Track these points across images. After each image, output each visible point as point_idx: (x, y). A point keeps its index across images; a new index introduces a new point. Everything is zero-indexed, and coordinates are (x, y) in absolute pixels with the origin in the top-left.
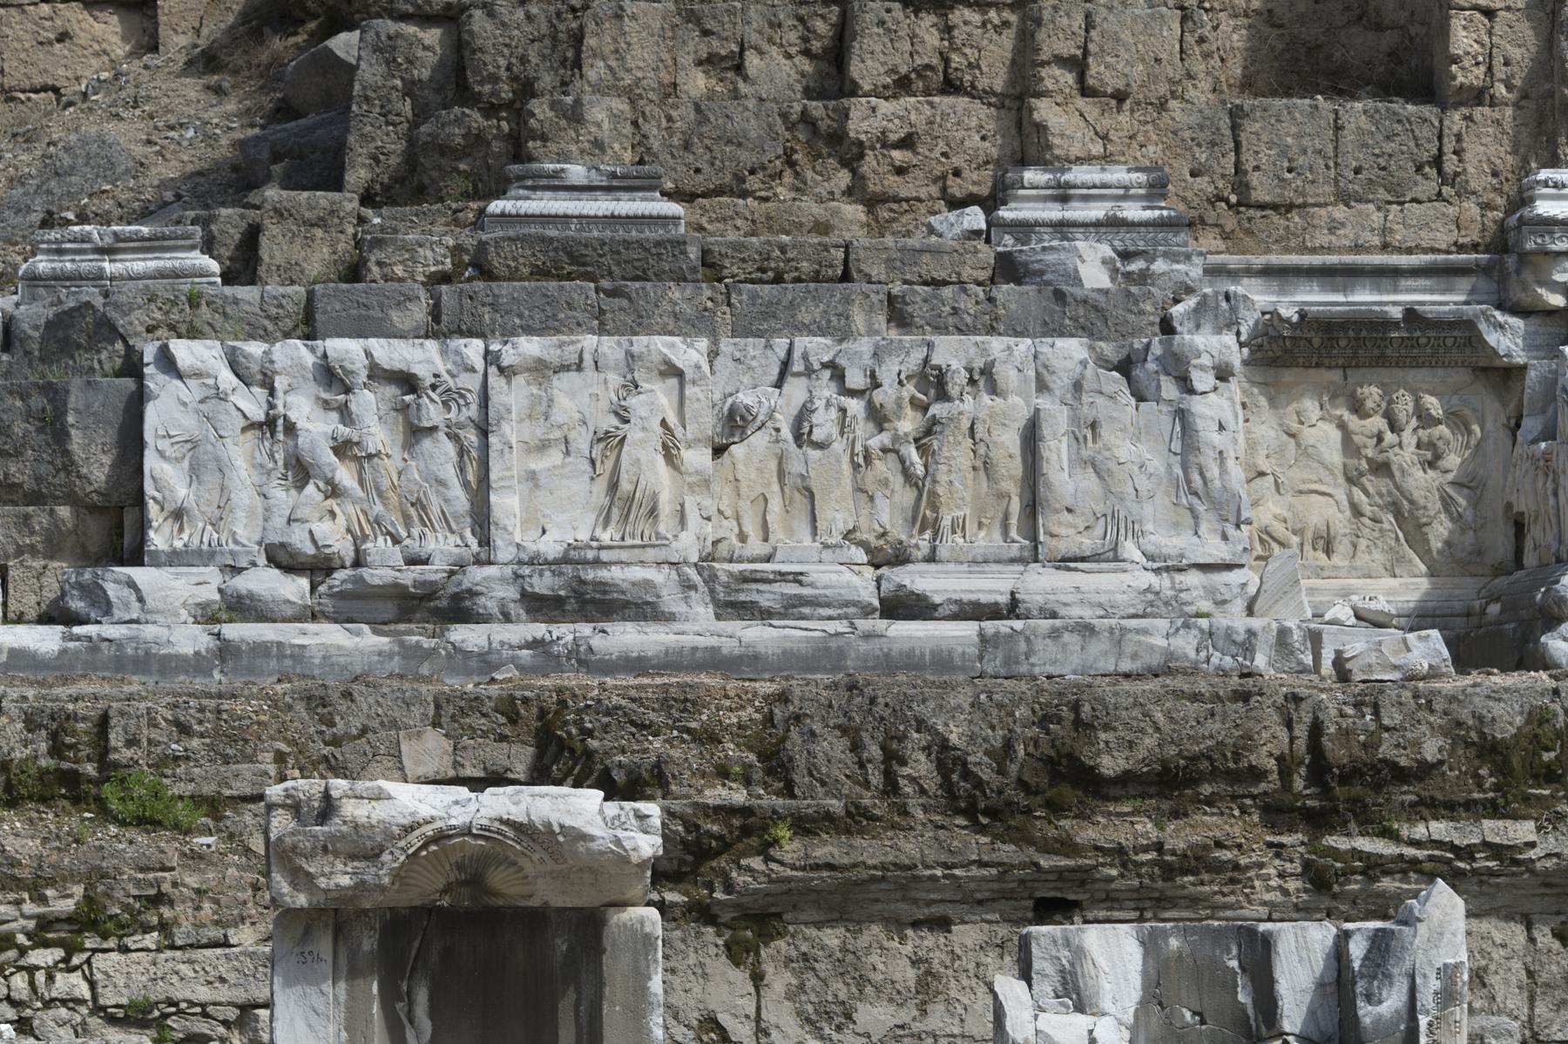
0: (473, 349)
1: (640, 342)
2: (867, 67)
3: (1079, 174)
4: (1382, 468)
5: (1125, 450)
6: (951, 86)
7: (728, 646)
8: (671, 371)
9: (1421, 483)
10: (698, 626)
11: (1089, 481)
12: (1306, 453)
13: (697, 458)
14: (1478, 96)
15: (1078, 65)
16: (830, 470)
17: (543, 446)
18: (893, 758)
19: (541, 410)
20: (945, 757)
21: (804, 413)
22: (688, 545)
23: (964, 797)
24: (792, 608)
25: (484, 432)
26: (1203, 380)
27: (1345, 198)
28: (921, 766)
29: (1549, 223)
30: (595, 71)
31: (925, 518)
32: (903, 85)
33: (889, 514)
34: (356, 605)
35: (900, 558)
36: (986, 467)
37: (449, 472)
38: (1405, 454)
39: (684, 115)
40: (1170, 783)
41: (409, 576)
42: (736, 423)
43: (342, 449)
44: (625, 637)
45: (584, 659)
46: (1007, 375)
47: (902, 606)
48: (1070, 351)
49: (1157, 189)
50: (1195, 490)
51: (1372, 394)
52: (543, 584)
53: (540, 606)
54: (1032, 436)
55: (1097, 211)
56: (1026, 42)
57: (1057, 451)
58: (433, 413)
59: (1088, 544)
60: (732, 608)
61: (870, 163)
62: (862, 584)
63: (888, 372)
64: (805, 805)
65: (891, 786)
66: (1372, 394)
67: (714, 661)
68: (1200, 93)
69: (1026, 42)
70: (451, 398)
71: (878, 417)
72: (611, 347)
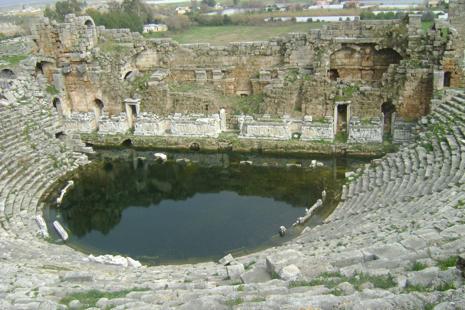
2: (278, 110)
33: (275, 133)
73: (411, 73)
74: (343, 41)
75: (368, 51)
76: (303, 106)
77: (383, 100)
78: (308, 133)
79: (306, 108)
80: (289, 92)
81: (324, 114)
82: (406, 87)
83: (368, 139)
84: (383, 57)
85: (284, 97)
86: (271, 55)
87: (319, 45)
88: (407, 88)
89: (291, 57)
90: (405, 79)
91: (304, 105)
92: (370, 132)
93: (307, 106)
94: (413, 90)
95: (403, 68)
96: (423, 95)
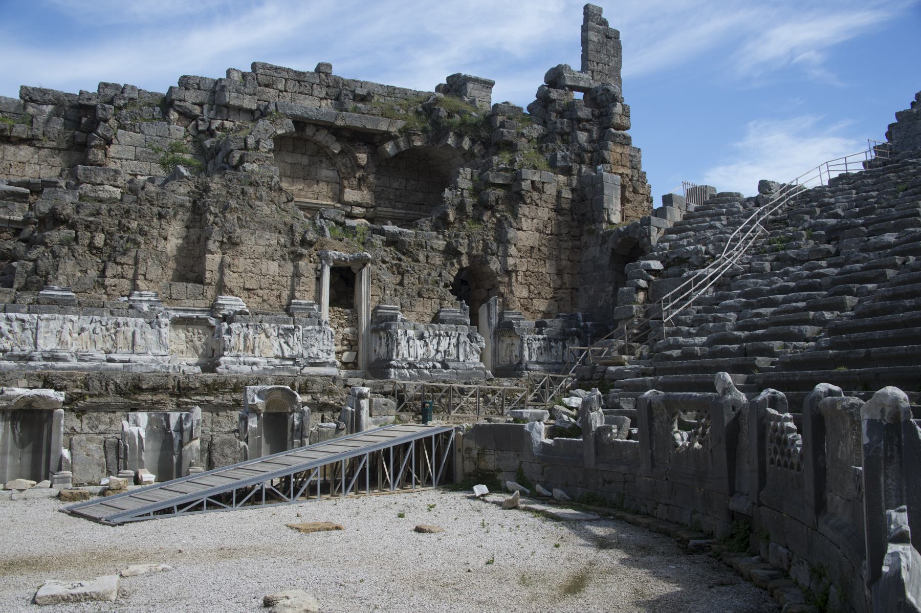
0: (36, 316)
1: (66, 316)
2: (109, 273)
3: (144, 292)
4: (192, 341)
5: (149, 337)
6: (123, 277)
7: (79, 366)
8: (71, 321)
9: (198, 343)
10: (74, 363)
11: (143, 341)
12: (179, 338)
13: (76, 335)
14: (210, 284)
15: (144, 275)
16: (99, 338)
17: (48, 332)
18: (107, 385)
19: (48, 326)
20: (116, 385)
21: (95, 329)
22: (73, 349)
23: (119, 391)
24: (91, 360)
25: (37, 329)
26: (163, 326)
27: (188, 299)
28: (112, 386)
29: (220, 304)
30: (61, 271)
31: (115, 346)
32: (115, 277)
33: (109, 345)
34: (11, 358)
35: (110, 353)
36: (126, 338)
37: (30, 336)
38: (196, 339)
39: (76, 279)
40: (154, 390)
41: (21, 353)
42: (82, 330)
43: (10, 331)
44: (61, 364)
45: (53, 368)
46: (130, 324)
47: (110, 360)
48: (141, 321)
49: (157, 296)
50: (161, 343)
51: (190, 329)
52: (46, 355)
53: (45, 359)
54: (134, 334)
55: (147, 299)
56: (136, 271)
57: (138, 336)
58: (27, 326)
59: (142, 351)
60: (80, 360)
61: (108, 289)
62: (104, 357)
63: (110, 323)
64: (91, 392)
65: (107, 390)
66: (190, 329)
67: (77, 369)
68: (165, 281)
69: (136, 271)
70: (31, 324)
71: (107, 330)
72: (61, 316)
73: (533, 182)
74: (299, 113)
75: (362, 158)
76: (213, 261)
77: (459, 263)
78: (250, 343)
79: (222, 266)
80: (155, 210)
81: (286, 293)
82: (523, 220)
83: (451, 365)
84: (396, 185)
85: (134, 225)
86: (29, 141)
87: (216, 123)
88: (525, 223)
89: (112, 150)
90: (515, 197)
91: (217, 257)
92: (454, 341)
93: (228, 259)
94: (538, 230)
95: (506, 170)
96: (565, 245)
